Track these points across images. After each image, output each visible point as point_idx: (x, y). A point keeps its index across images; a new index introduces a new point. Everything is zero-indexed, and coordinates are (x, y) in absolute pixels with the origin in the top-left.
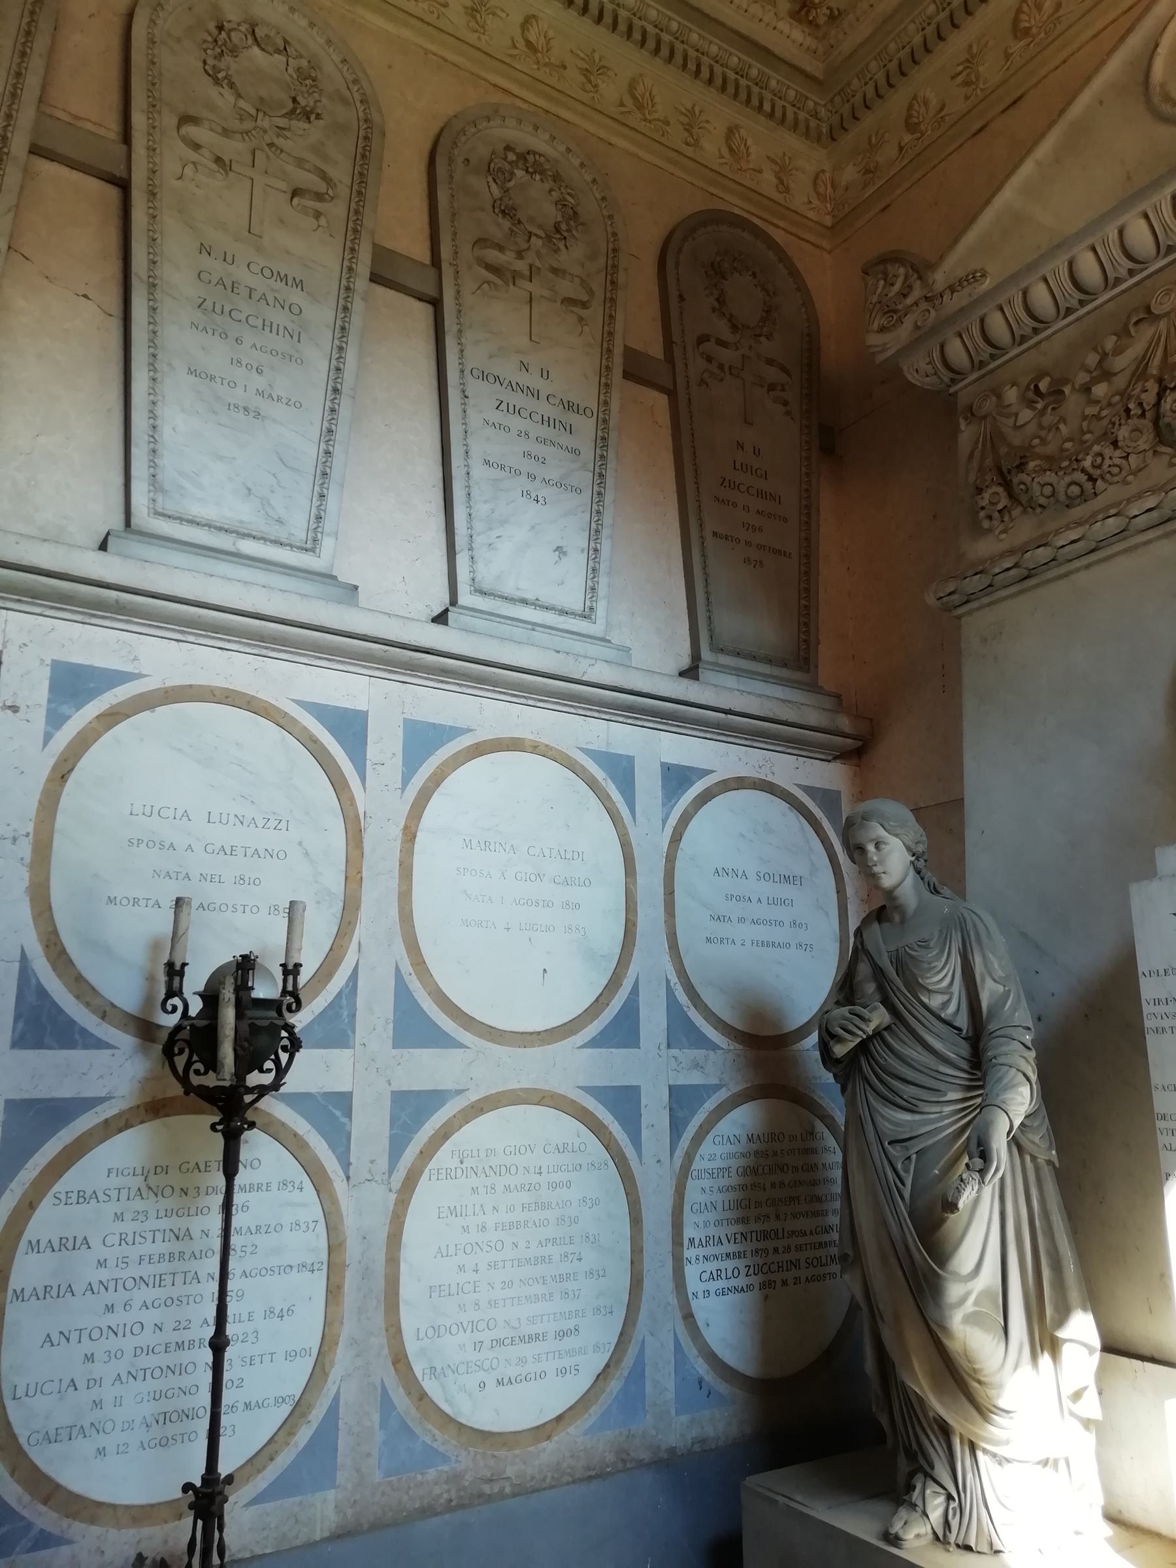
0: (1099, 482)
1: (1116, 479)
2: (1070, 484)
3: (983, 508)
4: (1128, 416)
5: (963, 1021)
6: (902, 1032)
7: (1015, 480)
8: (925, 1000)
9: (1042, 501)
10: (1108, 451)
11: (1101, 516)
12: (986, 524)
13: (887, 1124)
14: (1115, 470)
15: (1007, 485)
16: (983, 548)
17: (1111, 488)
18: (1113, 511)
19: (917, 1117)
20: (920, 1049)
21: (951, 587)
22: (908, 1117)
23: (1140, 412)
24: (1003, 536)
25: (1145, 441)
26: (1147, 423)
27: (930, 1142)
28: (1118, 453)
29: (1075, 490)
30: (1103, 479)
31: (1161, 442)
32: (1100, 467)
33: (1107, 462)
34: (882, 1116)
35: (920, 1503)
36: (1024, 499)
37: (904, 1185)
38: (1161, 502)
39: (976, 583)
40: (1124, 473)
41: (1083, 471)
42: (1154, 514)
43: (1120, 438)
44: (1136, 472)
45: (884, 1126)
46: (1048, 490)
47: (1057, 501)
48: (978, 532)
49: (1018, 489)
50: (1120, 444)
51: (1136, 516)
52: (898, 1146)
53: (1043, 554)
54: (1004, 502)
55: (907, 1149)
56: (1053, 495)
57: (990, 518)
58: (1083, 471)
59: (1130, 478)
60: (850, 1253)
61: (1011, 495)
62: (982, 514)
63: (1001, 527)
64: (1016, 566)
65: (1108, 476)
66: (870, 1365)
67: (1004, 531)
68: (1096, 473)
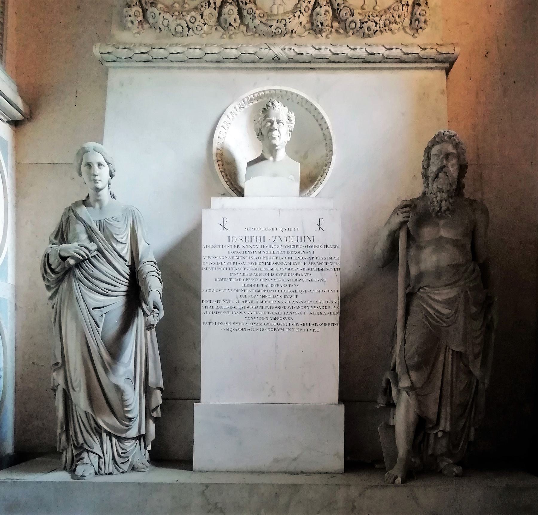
0: (191, 30)
1: (198, 33)
2: (178, 25)
3: (130, 16)
4: (209, 6)
7: (150, 10)
9: (161, 26)
10: (199, 17)
11: (193, 47)
12: (130, 25)
14: (199, 28)
15: (144, 11)
16: (125, 36)
17: (194, 35)
18: (198, 47)
21: (110, 49)
23: (214, 7)
24: (138, 35)
25: (213, 21)
26: (216, 13)
28: (202, 20)
29: (179, 29)
30: (193, 29)
31: (220, 25)
32: (193, 23)
33: (197, 23)
35: (88, 462)
36: (151, 20)
38: (220, 52)
39: (124, 53)
40: (202, 31)
41: (186, 21)
42: (216, 56)
43: (204, 14)
44: (207, 34)
46: (166, 23)
47: (169, 30)
48: (123, 27)
49: (149, 14)
50: (204, 17)
51: (208, 54)
53: (162, 53)
54: (141, 18)
56: (167, 26)
57: (132, 22)
58: (186, 21)
59: (205, 35)
61: (144, 16)
62: (129, 19)
63: (137, 30)
64: (147, 53)
65: (195, 30)
66: (60, 413)
67: (138, 33)
68: (191, 25)
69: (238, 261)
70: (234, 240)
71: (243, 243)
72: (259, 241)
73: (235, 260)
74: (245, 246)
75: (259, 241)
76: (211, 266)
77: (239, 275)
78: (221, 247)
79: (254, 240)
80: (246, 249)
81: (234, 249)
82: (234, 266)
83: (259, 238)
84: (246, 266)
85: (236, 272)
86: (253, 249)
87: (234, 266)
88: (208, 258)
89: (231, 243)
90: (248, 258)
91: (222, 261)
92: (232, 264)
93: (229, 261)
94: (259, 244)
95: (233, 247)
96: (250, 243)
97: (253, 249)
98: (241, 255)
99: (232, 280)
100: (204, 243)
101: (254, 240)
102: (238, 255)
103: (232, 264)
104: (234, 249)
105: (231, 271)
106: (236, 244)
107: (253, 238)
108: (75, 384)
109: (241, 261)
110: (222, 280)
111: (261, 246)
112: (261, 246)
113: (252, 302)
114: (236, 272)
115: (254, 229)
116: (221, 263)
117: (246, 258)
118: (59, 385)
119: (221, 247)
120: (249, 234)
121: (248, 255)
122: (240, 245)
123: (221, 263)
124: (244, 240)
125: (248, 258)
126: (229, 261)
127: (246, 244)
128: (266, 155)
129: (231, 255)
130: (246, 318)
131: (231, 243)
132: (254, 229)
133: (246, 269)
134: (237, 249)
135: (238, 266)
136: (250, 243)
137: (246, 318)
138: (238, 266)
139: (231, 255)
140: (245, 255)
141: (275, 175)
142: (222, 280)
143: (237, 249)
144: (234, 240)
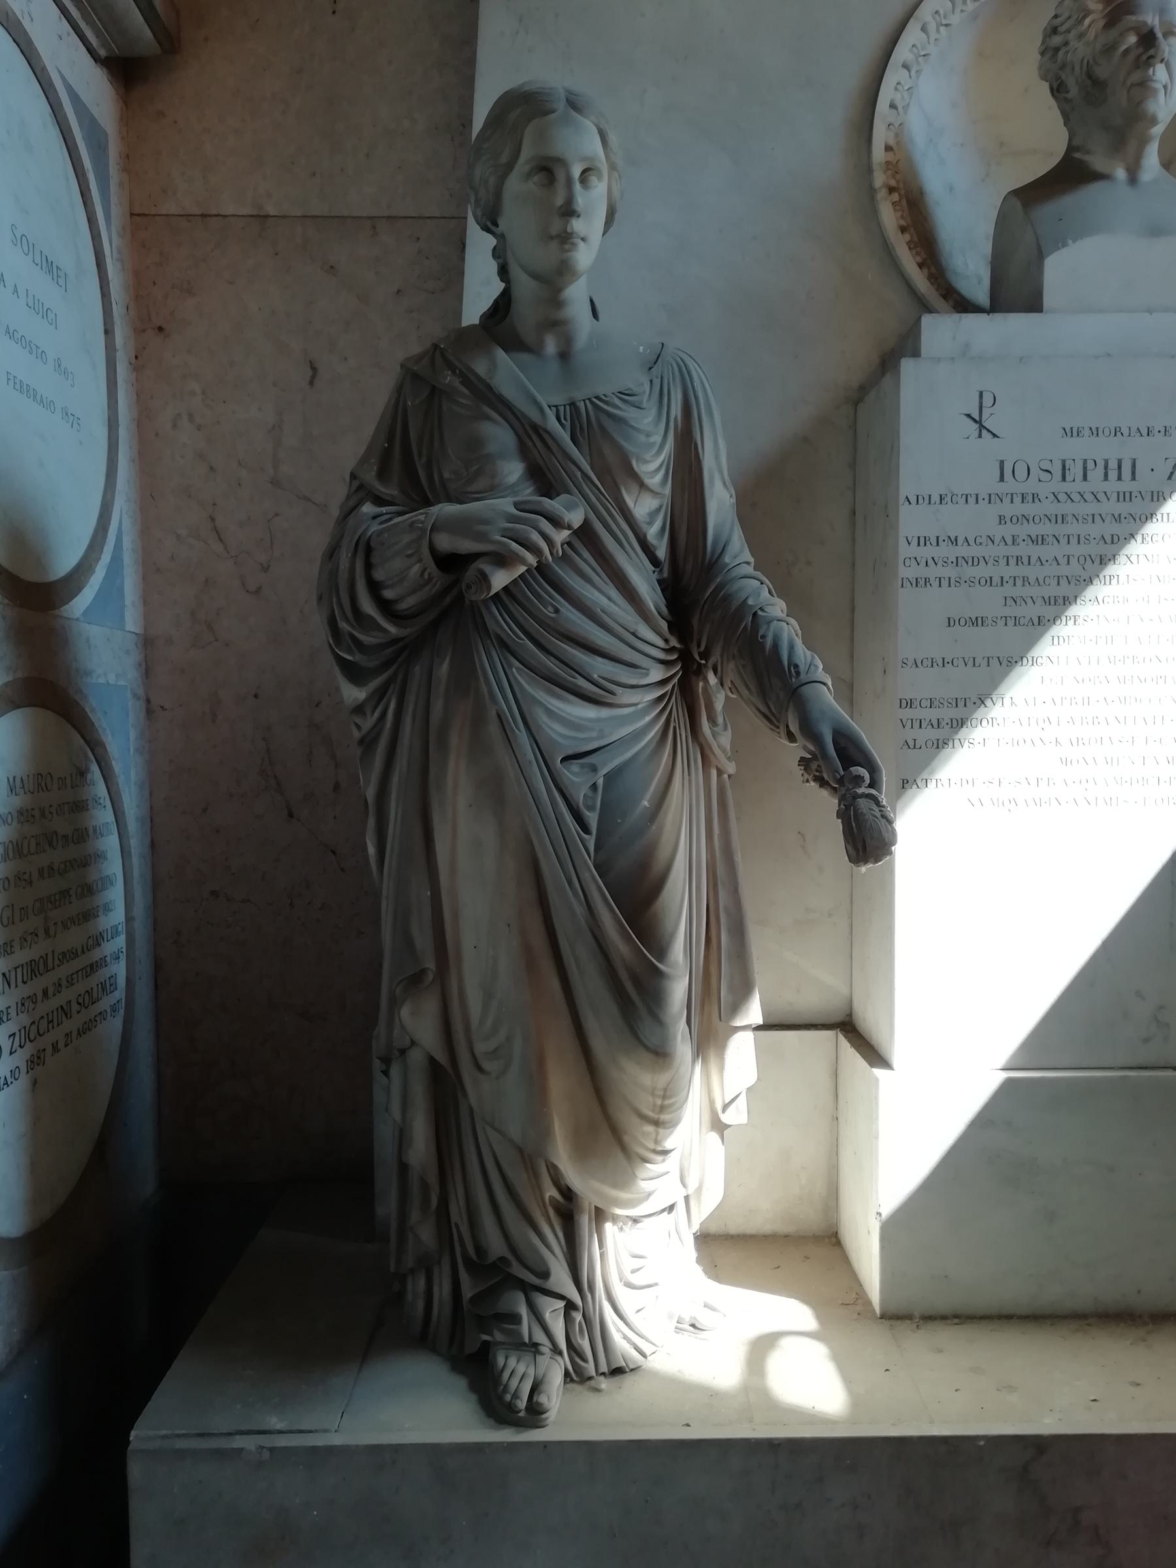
5: (662, 553)
6: (586, 560)
8: (629, 501)
13: (558, 727)
19: (605, 713)
20: (614, 593)
22: (589, 712)
27: (629, 755)
34: (550, 713)
37: (587, 830)
45: (554, 730)
52: (575, 766)
55: (594, 769)
60: (430, 964)
69: (1036, 551)
70: (1021, 472)
71: (1056, 485)
72: (1113, 475)
73: (1023, 549)
74: (1062, 497)
75: (1113, 475)
76: (933, 572)
77: (1039, 601)
78: (972, 500)
79: (1096, 474)
80: (1067, 508)
81: (1019, 508)
82: (1021, 571)
83: (1113, 465)
84: (1064, 570)
85: (1027, 591)
86: (1091, 508)
87: (1021, 571)
88: (922, 541)
89: (1010, 486)
90: (1074, 541)
91: (975, 551)
92: (1012, 562)
93: (1000, 550)
94: (1113, 486)
95: (1017, 500)
96: (1080, 486)
97: (1091, 508)
98: (1046, 529)
99: (1011, 622)
100: (907, 487)
101: (1096, 474)
102: (1035, 530)
103: (1012, 562)
104: (1019, 508)
105: (1008, 590)
106: (1031, 486)
107: (1090, 465)
108: (480, 1048)
109: (1048, 551)
110: (975, 622)
111: (1123, 497)
112: (1123, 497)
113: (1087, 701)
114: (1027, 591)
115: (1095, 432)
116: (974, 561)
117: (1064, 541)
118: (413, 1043)
119: (972, 500)
120: (1077, 449)
121: (1073, 528)
122: (1044, 490)
123: (974, 561)
124: (1057, 470)
125: (1074, 541)
126: (1000, 550)
127: (1067, 487)
128: (1097, 162)
129: (1008, 530)
130: (1065, 762)
131: (1010, 486)
132: (1095, 432)
133: (1064, 582)
134: (1029, 509)
135: (1032, 572)
136: (1080, 486)
137: (1065, 762)
138: (1032, 572)
139: (1008, 530)
140: (1061, 530)
141: (1156, 231)
142: (975, 622)
143: (1029, 509)
144: (1021, 472)
